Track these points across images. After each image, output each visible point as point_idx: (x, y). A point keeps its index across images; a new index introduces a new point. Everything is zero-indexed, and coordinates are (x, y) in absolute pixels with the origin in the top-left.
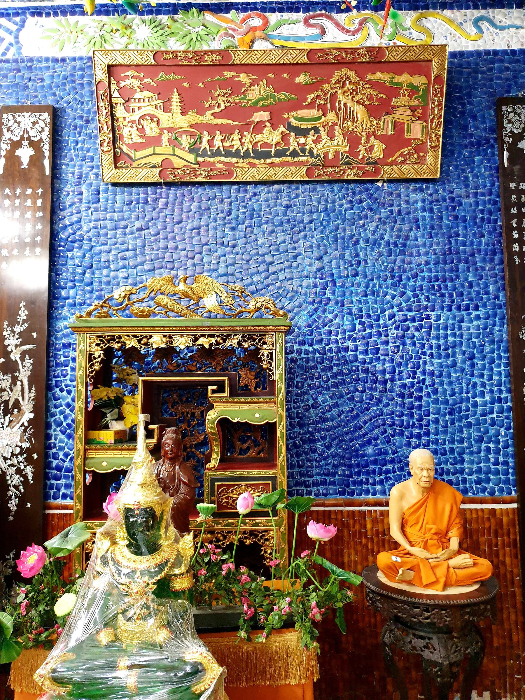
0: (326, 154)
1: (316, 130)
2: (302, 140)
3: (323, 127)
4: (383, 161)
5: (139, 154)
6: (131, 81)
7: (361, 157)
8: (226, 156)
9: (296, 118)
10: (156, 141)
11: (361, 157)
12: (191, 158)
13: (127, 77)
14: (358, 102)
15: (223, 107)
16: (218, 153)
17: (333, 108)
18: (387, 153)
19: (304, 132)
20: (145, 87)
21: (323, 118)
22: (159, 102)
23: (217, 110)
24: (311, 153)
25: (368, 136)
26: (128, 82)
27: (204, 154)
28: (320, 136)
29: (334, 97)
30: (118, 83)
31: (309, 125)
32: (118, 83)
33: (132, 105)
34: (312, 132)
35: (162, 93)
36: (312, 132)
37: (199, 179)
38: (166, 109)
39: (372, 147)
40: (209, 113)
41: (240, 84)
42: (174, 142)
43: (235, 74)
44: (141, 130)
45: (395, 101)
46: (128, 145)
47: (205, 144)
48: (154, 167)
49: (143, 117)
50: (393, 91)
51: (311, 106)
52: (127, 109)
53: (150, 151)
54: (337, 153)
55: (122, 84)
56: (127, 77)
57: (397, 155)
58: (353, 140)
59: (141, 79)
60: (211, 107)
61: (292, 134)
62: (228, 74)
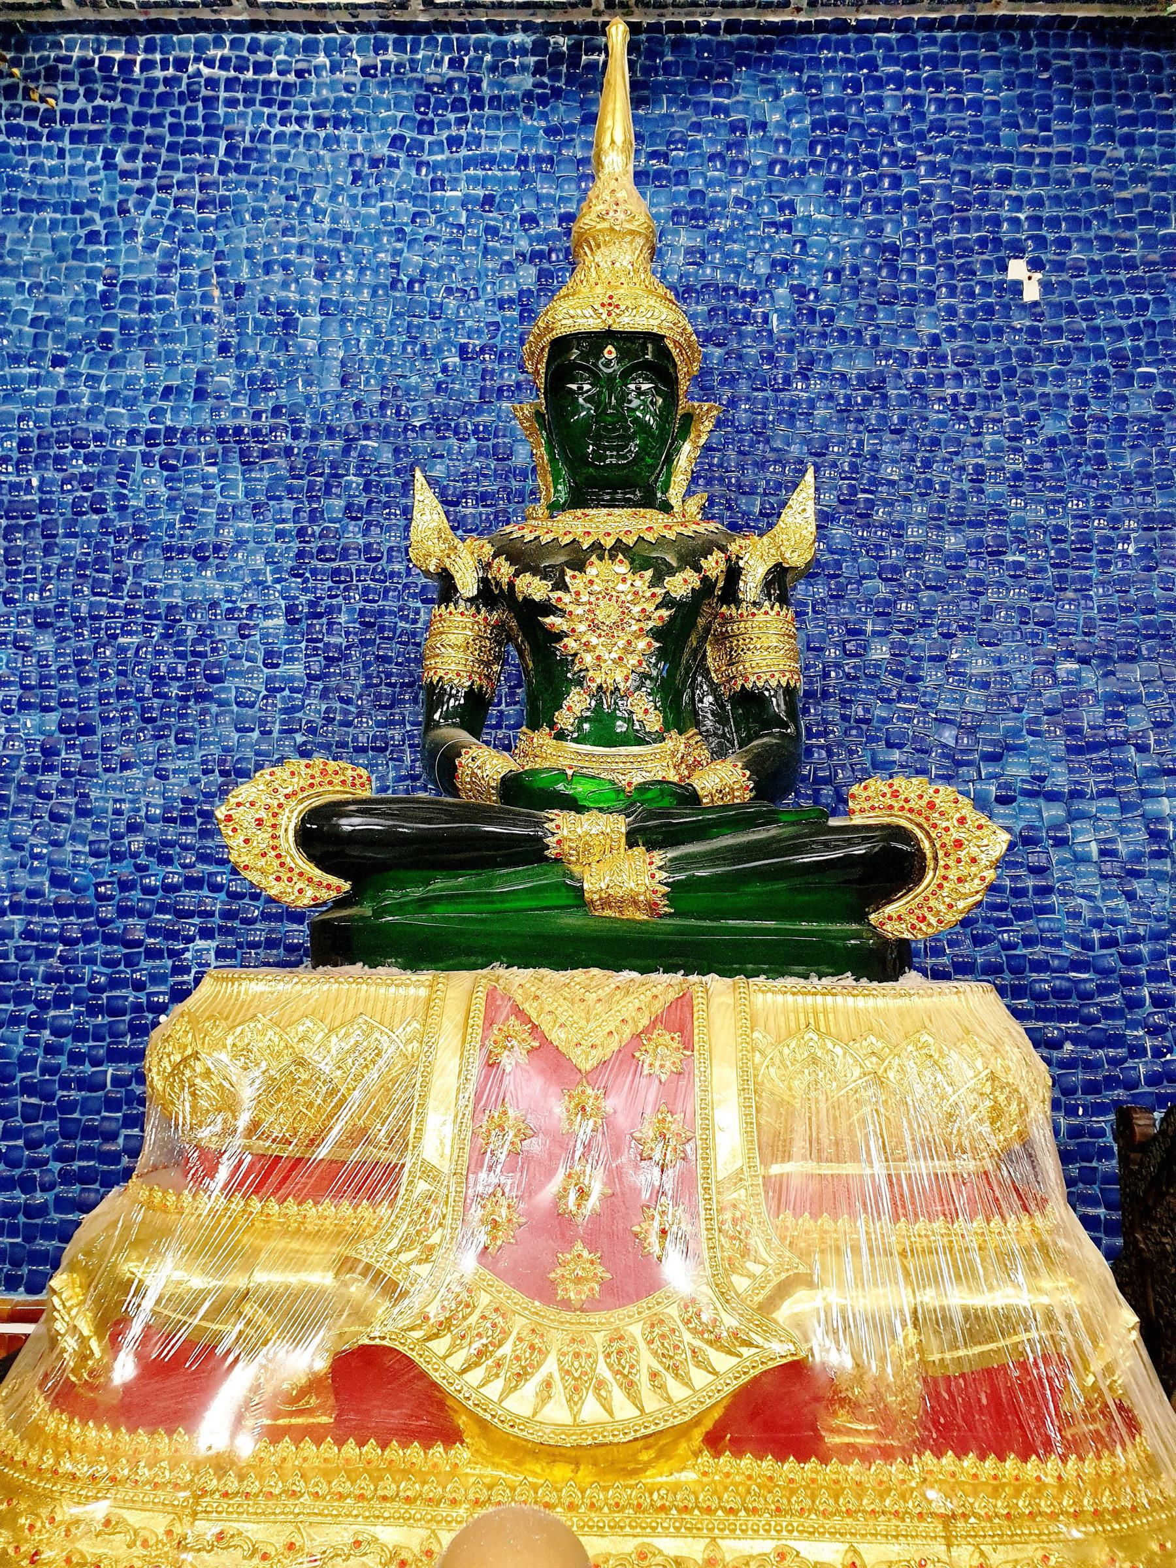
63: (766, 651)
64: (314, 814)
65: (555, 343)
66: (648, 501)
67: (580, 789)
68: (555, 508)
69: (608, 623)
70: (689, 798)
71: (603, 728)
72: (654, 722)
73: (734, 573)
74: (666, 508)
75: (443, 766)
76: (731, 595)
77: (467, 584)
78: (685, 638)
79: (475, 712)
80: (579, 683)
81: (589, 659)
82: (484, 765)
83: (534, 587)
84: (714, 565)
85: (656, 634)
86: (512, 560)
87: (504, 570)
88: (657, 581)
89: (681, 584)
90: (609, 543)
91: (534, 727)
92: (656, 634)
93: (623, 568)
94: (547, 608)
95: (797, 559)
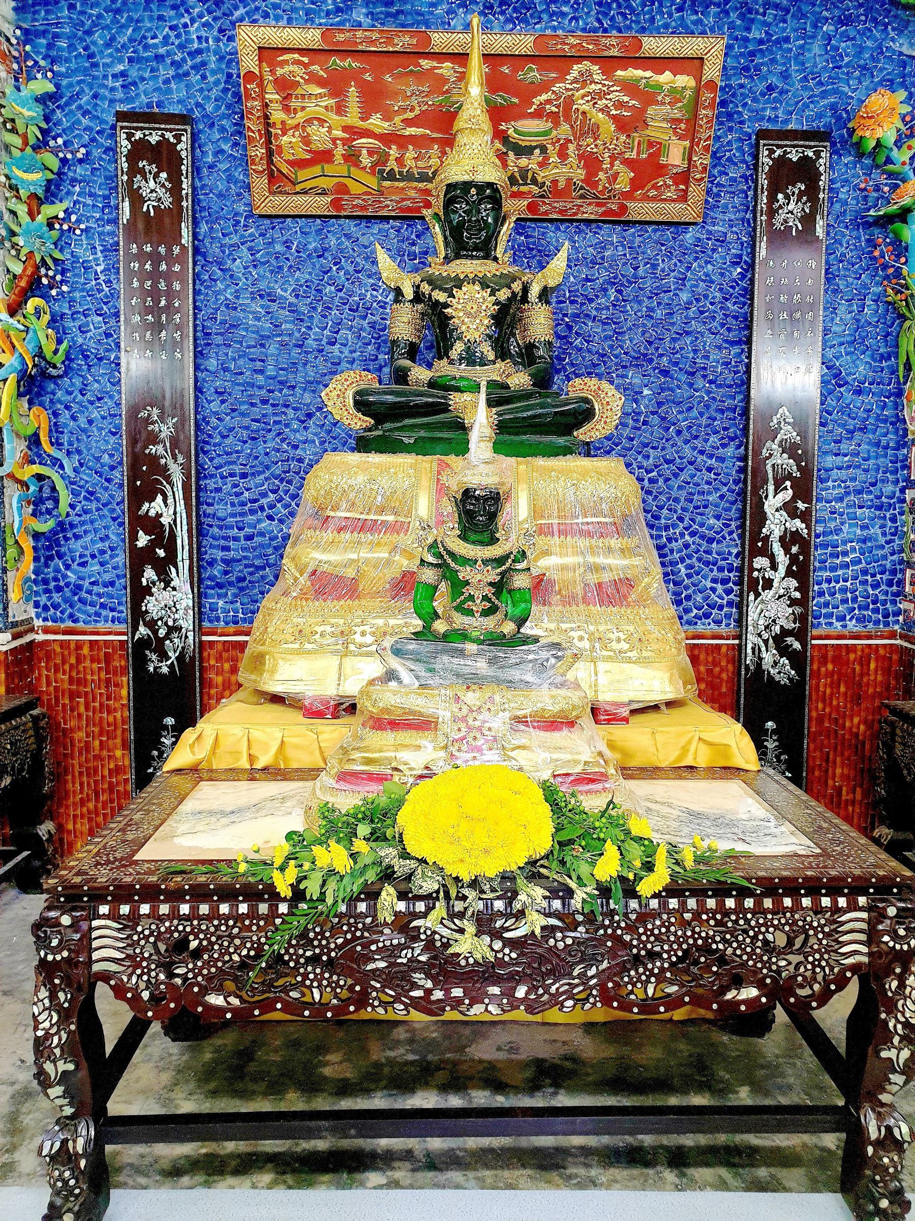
0: (555, 182)
1: (544, 149)
2: (523, 162)
3: (553, 144)
4: (628, 196)
5: (303, 174)
6: (291, 68)
7: (600, 188)
8: (420, 180)
9: (516, 131)
10: (324, 157)
11: (600, 188)
12: (373, 182)
13: (286, 62)
14: (601, 110)
15: (417, 112)
16: (409, 177)
17: (567, 118)
18: (636, 185)
19: (527, 151)
20: (314, 79)
21: (554, 133)
22: (332, 102)
23: (410, 115)
24: (534, 181)
25: (613, 158)
26: (287, 69)
27: (391, 176)
28: (547, 158)
29: (570, 101)
30: (272, 72)
31: (533, 141)
32: (272, 72)
33: (294, 103)
34: (537, 151)
35: (335, 85)
36: (537, 151)
37: (384, 213)
38: (340, 109)
39: (615, 176)
40: (397, 119)
41: (444, 80)
42: (352, 158)
43: (435, 64)
44: (306, 140)
45: (651, 111)
46: (287, 162)
47: (392, 164)
48: (324, 193)
49: (309, 121)
50: (648, 97)
51: (538, 114)
52: (286, 109)
53: (316, 170)
54: (569, 180)
55: (280, 71)
56: (286, 62)
57: (649, 185)
58: (591, 163)
59: (305, 66)
60: (404, 110)
61: (511, 154)
62: (425, 63)
63: (539, 324)
64: (357, 393)
65: (448, 186)
66: (486, 257)
67: (462, 384)
68: (447, 260)
69: (471, 313)
70: (507, 387)
71: (470, 358)
72: (491, 356)
73: (526, 289)
74: (496, 259)
75: (401, 376)
76: (525, 299)
77: (409, 293)
78: (506, 318)
79: (413, 352)
80: (460, 338)
81: (464, 328)
82: (420, 374)
83: (441, 297)
84: (517, 287)
85: (493, 317)
86: (429, 283)
87: (426, 288)
88: (493, 294)
89: (503, 295)
90: (471, 276)
91: (440, 358)
92: (493, 317)
93: (477, 287)
94: (446, 305)
95: (552, 283)
